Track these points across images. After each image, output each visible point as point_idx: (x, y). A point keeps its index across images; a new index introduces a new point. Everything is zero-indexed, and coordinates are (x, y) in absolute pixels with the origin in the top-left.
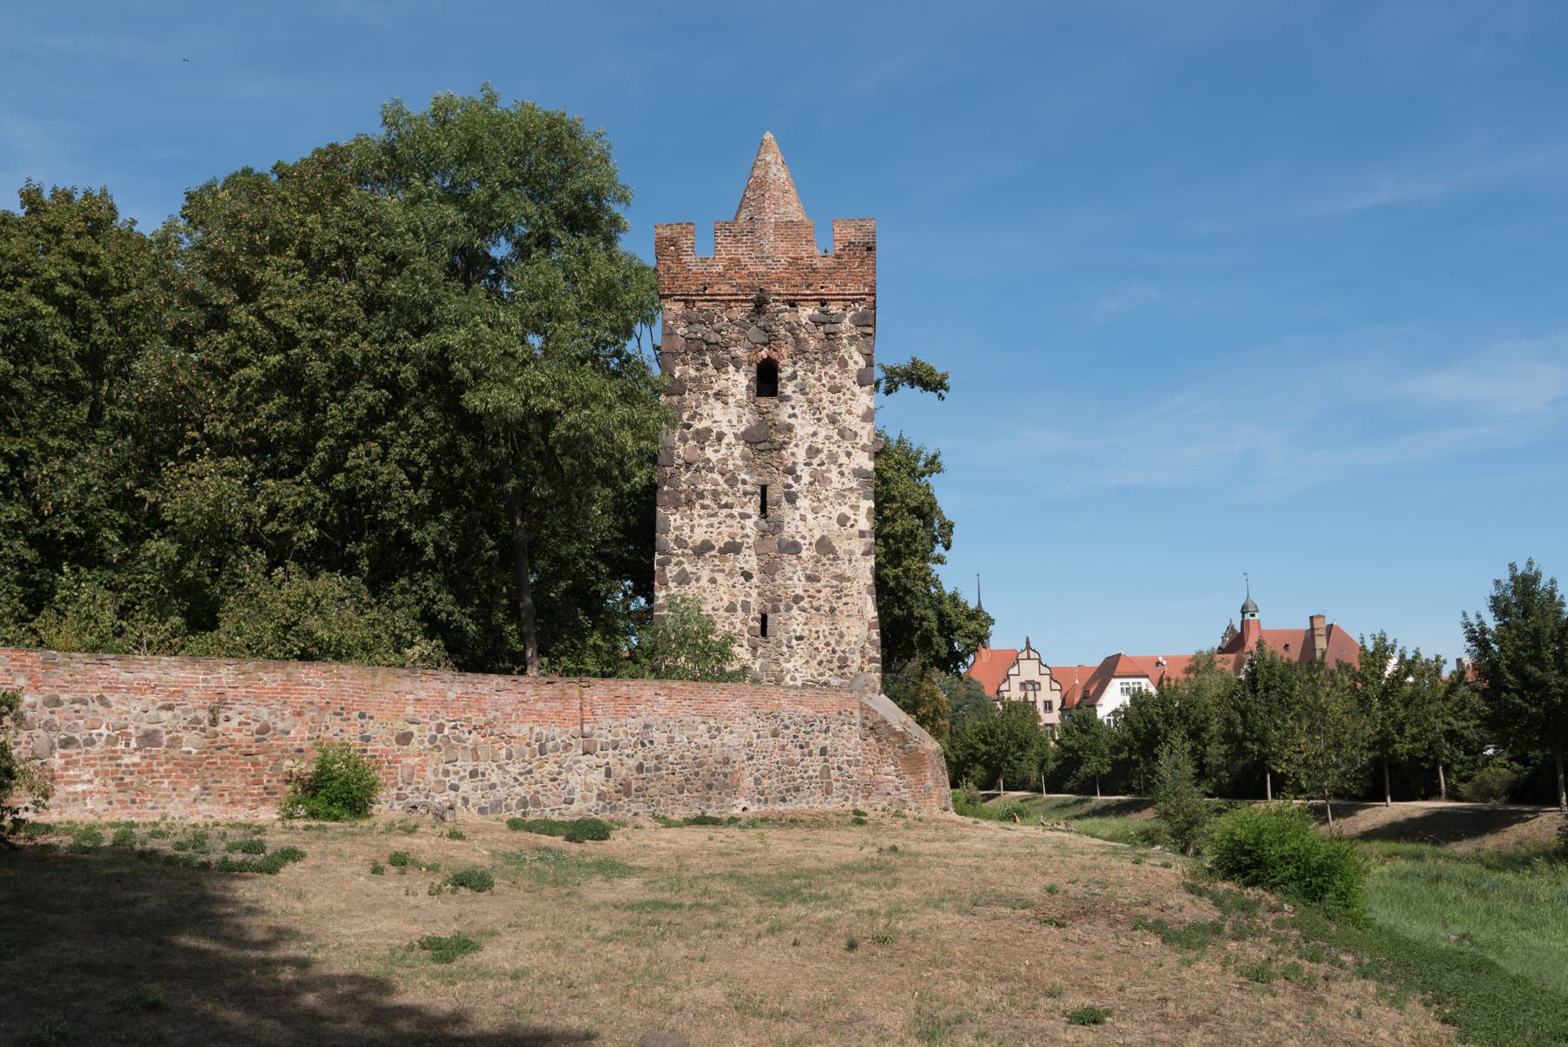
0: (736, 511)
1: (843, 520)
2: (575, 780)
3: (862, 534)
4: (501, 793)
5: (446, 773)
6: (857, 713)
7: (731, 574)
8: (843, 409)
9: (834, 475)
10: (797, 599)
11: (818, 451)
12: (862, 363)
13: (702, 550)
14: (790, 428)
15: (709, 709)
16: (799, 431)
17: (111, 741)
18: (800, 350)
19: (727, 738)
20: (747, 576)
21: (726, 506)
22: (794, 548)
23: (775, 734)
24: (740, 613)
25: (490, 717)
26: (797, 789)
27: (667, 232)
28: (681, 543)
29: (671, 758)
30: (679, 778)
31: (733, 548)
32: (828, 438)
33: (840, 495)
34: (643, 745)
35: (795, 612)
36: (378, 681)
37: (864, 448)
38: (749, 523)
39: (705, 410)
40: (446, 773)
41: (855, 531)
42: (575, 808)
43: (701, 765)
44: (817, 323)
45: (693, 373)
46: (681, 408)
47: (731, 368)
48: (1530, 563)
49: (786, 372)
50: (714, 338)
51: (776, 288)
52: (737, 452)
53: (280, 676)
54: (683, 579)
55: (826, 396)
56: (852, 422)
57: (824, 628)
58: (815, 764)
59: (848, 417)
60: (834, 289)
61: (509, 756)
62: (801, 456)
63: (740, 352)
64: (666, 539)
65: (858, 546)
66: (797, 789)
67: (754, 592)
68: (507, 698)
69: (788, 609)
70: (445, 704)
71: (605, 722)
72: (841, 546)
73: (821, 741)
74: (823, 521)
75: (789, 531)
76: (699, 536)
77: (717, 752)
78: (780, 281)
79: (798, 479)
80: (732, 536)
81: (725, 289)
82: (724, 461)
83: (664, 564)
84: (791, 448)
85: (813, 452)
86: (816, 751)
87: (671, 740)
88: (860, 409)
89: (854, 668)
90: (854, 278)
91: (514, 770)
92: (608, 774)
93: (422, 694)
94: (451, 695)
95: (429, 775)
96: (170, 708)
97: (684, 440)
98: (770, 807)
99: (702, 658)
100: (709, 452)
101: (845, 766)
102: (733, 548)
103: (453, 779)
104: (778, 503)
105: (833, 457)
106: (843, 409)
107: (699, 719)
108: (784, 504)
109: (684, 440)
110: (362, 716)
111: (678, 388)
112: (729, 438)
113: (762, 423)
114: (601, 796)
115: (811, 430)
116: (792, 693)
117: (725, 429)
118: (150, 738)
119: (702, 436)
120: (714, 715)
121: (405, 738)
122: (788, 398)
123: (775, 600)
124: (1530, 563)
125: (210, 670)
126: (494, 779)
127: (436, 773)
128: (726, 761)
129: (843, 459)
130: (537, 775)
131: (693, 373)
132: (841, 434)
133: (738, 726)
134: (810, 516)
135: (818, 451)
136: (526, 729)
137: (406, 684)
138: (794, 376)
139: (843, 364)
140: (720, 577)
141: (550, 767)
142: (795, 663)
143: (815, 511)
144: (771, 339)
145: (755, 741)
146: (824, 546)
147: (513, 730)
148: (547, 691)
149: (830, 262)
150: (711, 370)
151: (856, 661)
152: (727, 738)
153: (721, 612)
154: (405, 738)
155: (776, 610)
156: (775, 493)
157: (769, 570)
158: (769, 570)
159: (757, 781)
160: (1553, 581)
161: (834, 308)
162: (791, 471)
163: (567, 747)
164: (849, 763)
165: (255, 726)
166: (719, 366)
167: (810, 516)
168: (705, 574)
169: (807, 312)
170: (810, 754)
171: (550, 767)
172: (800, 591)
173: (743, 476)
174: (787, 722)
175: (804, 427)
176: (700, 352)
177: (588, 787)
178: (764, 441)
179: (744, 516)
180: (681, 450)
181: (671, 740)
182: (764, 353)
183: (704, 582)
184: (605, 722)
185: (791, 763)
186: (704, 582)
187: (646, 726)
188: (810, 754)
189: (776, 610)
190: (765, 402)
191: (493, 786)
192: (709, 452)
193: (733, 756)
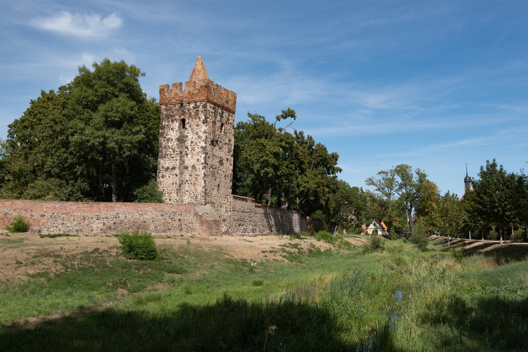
0: (175, 159)
1: (198, 160)
3: (202, 163)
6: (192, 210)
7: (173, 175)
8: (199, 131)
9: (196, 148)
10: (187, 181)
11: (193, 142)
12: (204, 118)
13: (167, 169)
14: (187, 136)
15: (139, 209)
16: (189, 137)
18: (190, 115)
19: (145, 216)
20: (177, 175)
21: (173, 157)
22: (187, 168)
23: (162, 215)
24: (175, 185)
25: (68, 211)
26: (170, 229)
27: (162, 88)
28: (163, 167)
30: (127, 226)
31: (174, 168)
32: (195, 138)
33: (198, 153)
34: (116, 218)
35: (187, 184)
36: (36, 203)
37: (203, 141)
38: (177, 162)
39: (169, 133)
41: (200, 163)
43: (136, 223)
44: (194, 108)
45: (167, 123)
46: (164, 133)
47: (175, 122)
48: (494, 160)
49: (187, 122)
50: (172, 114)
51: (185, 100)
52: (175, 144)
53: (10, 202)
54: (163, 177)
55: (196, 127)
56: (201, 134)
57: (193, 188)
58: (177, 223)
59: (200, 133)
60: (198, 99)
62: (189, 144)
63: (177, 117)
64: (160, 167)
65: (201, 167)
66: (170, 229)
67: (178, 180)
68: (73, 207)
69: (185, 183)
72: (197, 167)
73: (179, 217)
74: (194, 160)
75: (186, 163)
76: (167, 166)
78: (186, 98)
79: (188, 150)
80: (174, 165)
81: (174, 101)
82: (172, 146)
83: (159, 173)
84: (187, 142)
85: (192, 142)
86: (177, 220)
87: (126, 217)
88: (203, 131)
89: (199, 198)
90: (202, 95)
92: (104, 224)
97: (164, 141)
98: (160, 234)
99: (156, 197)
100: (169, 144)
101: (188, 224)
102: (174, 168)
104: (184, 156)
105: (196, 143)
106: (199, 131)
107: (135, 212)
108: (185, 156)
109: (164, 141)
110: (31, 211)
111: (163, 128)
112: (174, 140)
113: (181, 135)
115: (191, 137)
116: (169, 205)
117: (173, 138)
119: (168, 140)
120: (141, 211)
122: (187, 129)
123: (182, 181)
124: (494, 160)
128: (145, 222)
129: (199, 144)
131: (167, 123)
132: (198, 137)
133: (149, 214)
134: (191, 159)
135: (193, 142)
138: (188, 123)
139: (200, 118)
140: (171, 176)
142: (186, 197)
143: (192, 158)
144: (184, 113)
146: (194, 167)
148: (86, 205)
149: (197, 91)
150: (170, 123)
151: (199, 196)
152: (145, 216)
153: (171, 185)
155: (182, 184)
156: (184, 153)
157: (181, 173)
158: (181, 173)
159: (155, 227)
160: (501, 166)
161: (198, 104)
162: (187, 148)
165: (4, 213)
166: (172, 121)
167: (191, 159)
168: (168, 175)
169: (192, 105)
170: (175, 221)
172: (188, 179)
173: (176, 150)
174: (167, 212)
175: (190, 136)
176: (169, 118)
178: (181, 140)
179: (176, 160)
180: (163, 144)
181: (126, 217)
182: (182, 117)
183: (167, 177)
184: (104, 213)
186: (167, 177)
187: (117, 213)
188: (175, 221)
189: (182, 184)
190: (182, 130)
192: (169, 144)
193: (147, 221)
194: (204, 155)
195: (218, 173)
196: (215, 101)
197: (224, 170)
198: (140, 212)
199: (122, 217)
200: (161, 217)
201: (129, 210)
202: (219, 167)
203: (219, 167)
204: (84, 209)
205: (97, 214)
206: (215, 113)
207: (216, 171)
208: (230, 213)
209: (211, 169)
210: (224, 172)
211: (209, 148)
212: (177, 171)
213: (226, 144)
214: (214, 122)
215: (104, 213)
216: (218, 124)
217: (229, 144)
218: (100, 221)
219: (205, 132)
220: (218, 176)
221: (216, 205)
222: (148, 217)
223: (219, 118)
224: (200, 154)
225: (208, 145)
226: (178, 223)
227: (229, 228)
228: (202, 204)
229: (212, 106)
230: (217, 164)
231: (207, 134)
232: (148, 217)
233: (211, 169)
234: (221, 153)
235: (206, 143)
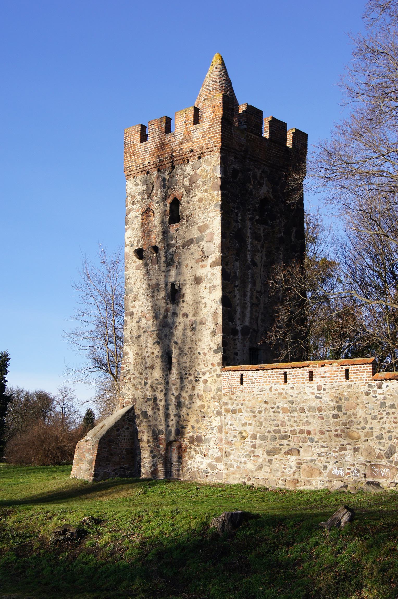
227: (218, 460)
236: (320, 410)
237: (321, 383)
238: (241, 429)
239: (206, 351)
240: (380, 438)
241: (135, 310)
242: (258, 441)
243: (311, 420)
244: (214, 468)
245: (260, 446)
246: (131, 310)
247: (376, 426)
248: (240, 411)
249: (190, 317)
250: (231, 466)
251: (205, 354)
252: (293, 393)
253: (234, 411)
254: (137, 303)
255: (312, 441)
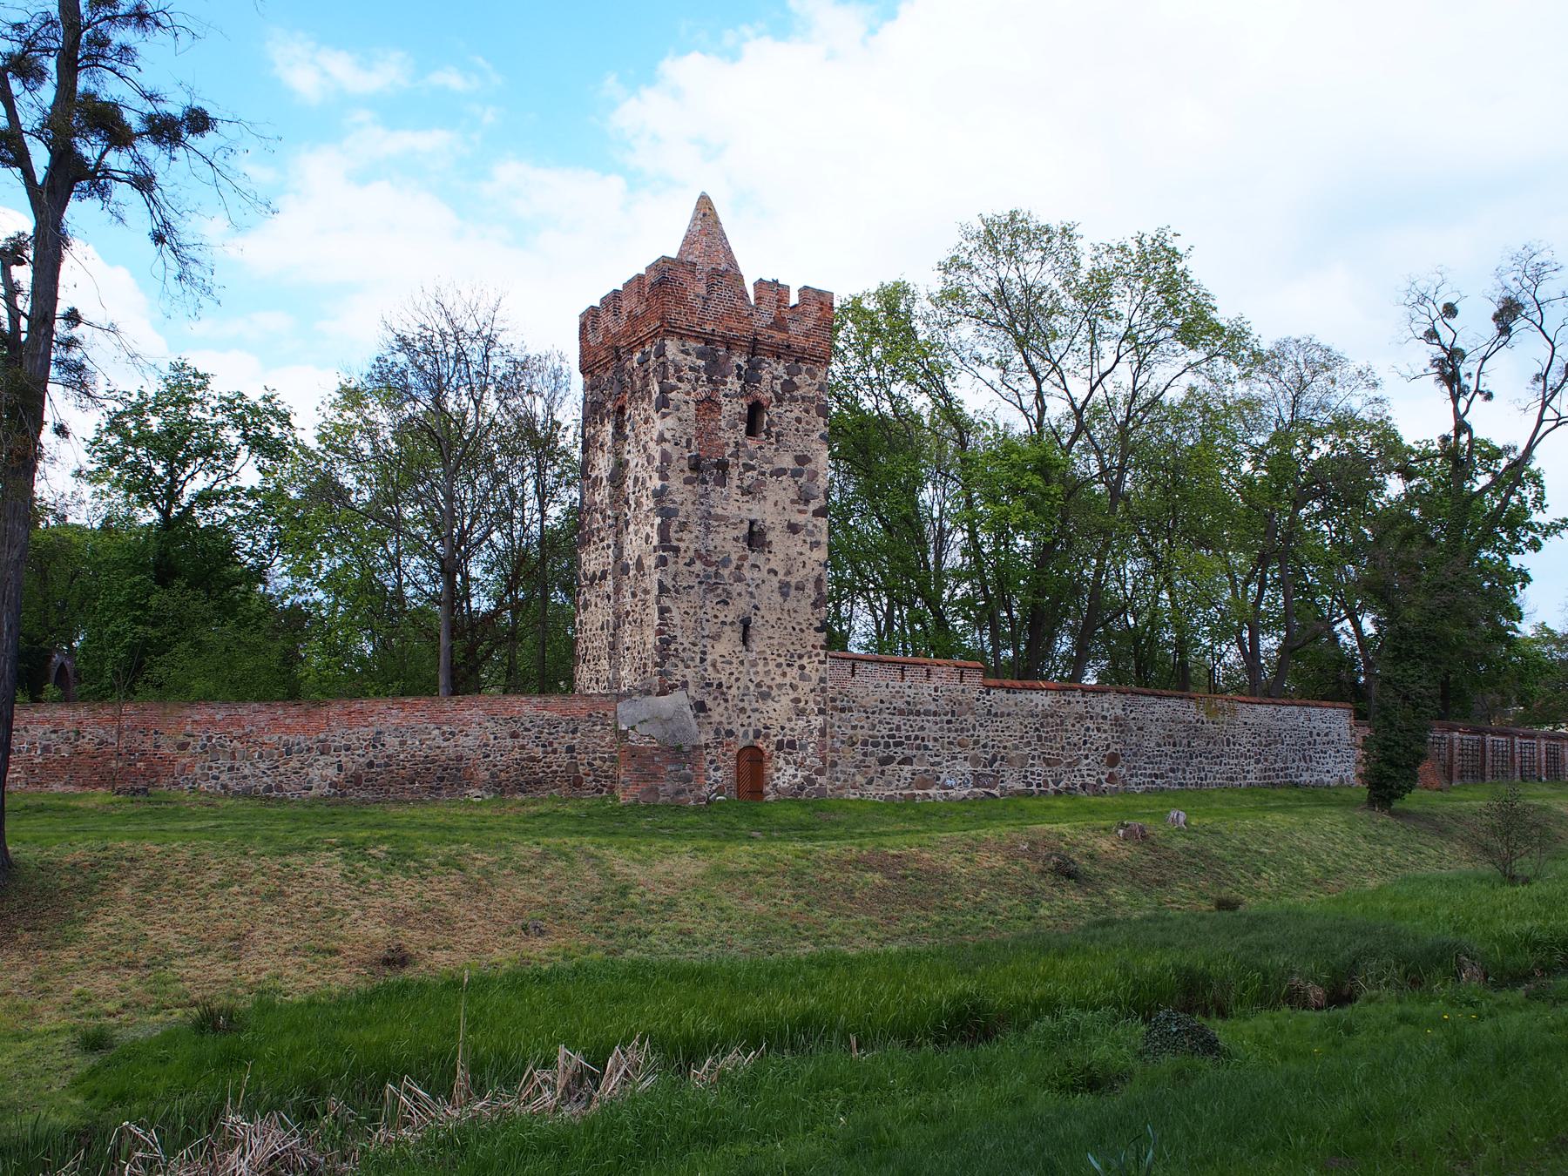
2: (315, 773)
4: (252, 782)
5: (210, 768)
10: (628, 613)
15: (443, 718)
16: (632, 465)
17: (29, 751)
19: (461, 740)
20: (609, 597)
23: (514, 735)
29: (402, 757)
34: (374, 747)
38: (610, 552)
40: (210, 768)
42: (312, 793)
43: (434, 761)
61: (261, 756)
70: (213, 723)
71: (339, 732)
77: (451, 752)
85: (636, 479)
87: (403, 743)
91: (262, 766)
92: (340, 768)
93: (197, 718)
94: (218, 717)
95: (197, 770)
96: (55, 732)
101: (598, 763)
103: (215, 772)
114: (331, 785)
118: (46, 749)
121: (183, 746)
125: (75, 710)
126: (246, 772)
127: (202, 768)
128: (460, 758)
130: (282, 770)
133: (474, 730)
136: (276, 738)
137: (187, 711)
141: (294, 764)
145: (492, 742)
147: (266, 738)
148: (293, 711)
150: (599, 427)
154: (183, 746)
159: (493, 775)
162: (627, 502)
163: (309, 750)
164: (604, 760)
168: (593, 600)
170: (555, 751)
171: (294, 764)
174: (528, 725)
177: (324, 778)
181: (403, 743)
185: (533, 759)
187: (379, 733)
188: (555, 751)
191: (245, 777)
194: (658, 520)
195: (739, 579)
196: (709, 328)
197: (773, 565)
198: (445, 728)
199: (392, 742)
200: (509, 742)
201: (412, 723)
202: (743, 558)
203: (743, 558)
204: (288, 721)
205: (322, 736)
206: (715, 370)
207: (725, 572)
208: (818, 721)
209: (698, 566)
210: (774, 572)
211: (680, 491)
212: (609, 585)
213: (779, 472)
214: (708, 405)
215: (339, 732)
216: (734, 408)
217: (796, 474)
218: (331, 760)
219: (662, 439)
220: (738, 587)
221: (734, 691)
222: (470, 741)
223: (733, 384)
224: (651, 515)
225: (675, 483)
226: (564, 758)
227: (820, 772)
228: (648, 693)
229: (692, 345)
230: (734, 551)
231: (666, 446)
232: (467, 743)
233: (698, 566)
234: (755, 506)
235: (664, 477)
236: (935, 714)
237: (939, 684)
238: (850, 732)
239: (804, 627)
240: (985, 746)
241: (682, 545)
242: (870, 748)
243: (927, 725)
244: (812, 782)
245: (872, 754)
246: (675, 543)
247: (983, 734)
248: (850, 710)
249: (781, 576)
250: (838, 779)
251: (802, 631)
252: (911, 692)
253: (843, 710)
254: (685, 535)
255: (926, 748)
